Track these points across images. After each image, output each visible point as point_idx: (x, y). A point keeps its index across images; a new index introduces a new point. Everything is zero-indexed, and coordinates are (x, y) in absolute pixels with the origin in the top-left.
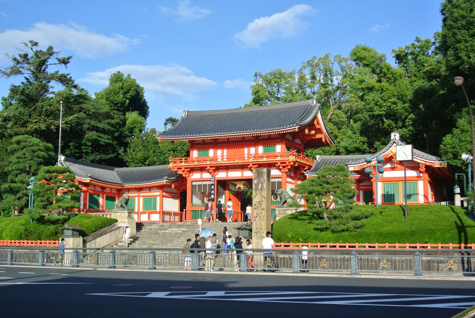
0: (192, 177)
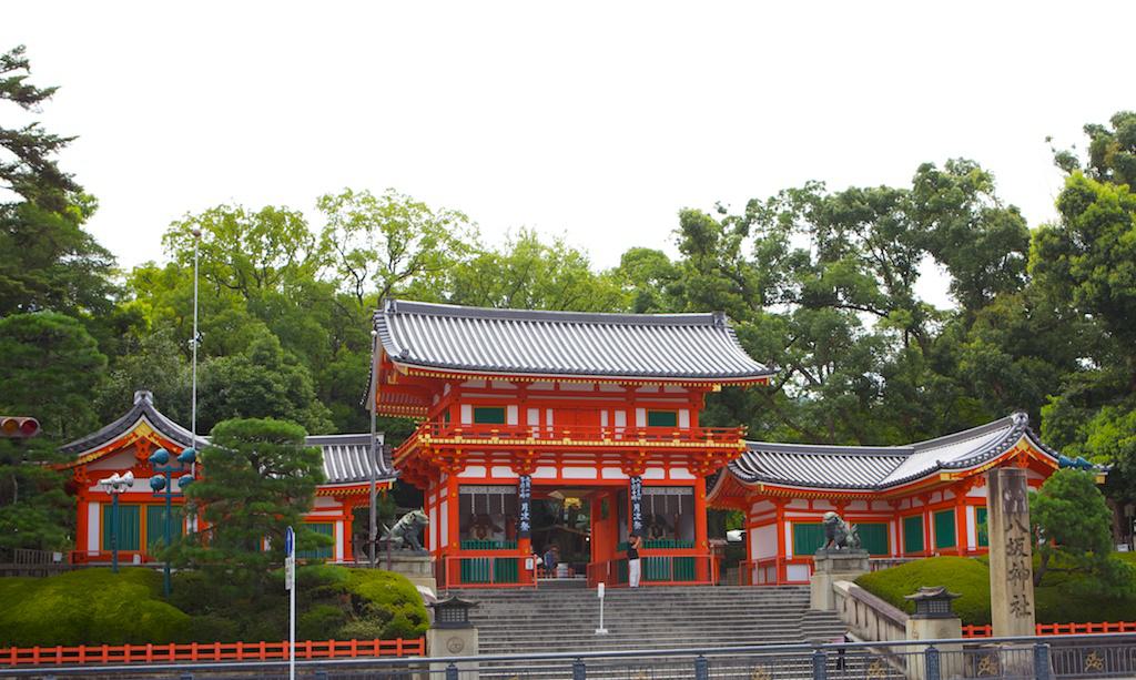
0: (460, 475)
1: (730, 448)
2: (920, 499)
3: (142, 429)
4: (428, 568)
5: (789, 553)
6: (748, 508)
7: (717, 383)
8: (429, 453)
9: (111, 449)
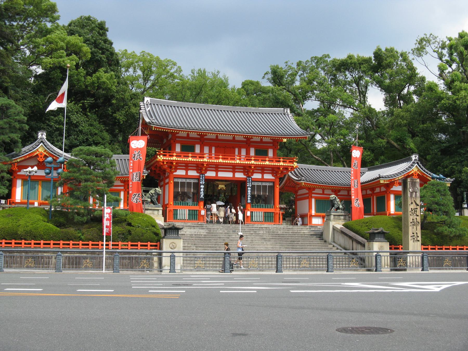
0: (175, 173)
1: (290, 166)
2: (370, 190)
3: (40, 149)
4: (161, 212)
5: (313, 212)
6: (296, 192)
7: (285, 138)
8: (162, 164)
9: (28, 157)
